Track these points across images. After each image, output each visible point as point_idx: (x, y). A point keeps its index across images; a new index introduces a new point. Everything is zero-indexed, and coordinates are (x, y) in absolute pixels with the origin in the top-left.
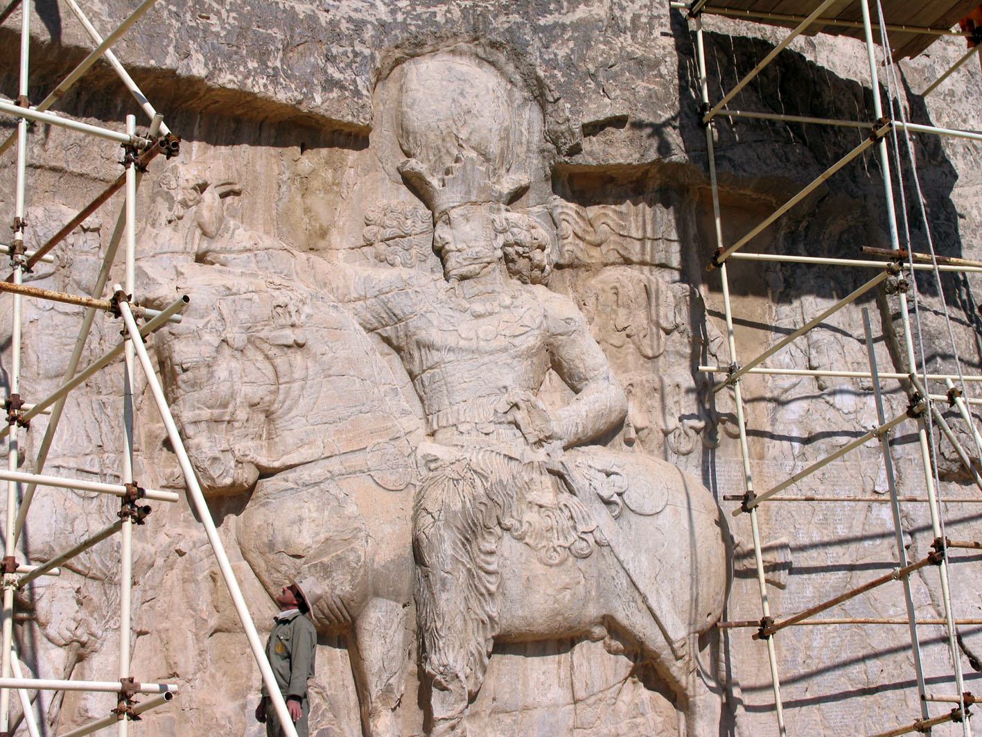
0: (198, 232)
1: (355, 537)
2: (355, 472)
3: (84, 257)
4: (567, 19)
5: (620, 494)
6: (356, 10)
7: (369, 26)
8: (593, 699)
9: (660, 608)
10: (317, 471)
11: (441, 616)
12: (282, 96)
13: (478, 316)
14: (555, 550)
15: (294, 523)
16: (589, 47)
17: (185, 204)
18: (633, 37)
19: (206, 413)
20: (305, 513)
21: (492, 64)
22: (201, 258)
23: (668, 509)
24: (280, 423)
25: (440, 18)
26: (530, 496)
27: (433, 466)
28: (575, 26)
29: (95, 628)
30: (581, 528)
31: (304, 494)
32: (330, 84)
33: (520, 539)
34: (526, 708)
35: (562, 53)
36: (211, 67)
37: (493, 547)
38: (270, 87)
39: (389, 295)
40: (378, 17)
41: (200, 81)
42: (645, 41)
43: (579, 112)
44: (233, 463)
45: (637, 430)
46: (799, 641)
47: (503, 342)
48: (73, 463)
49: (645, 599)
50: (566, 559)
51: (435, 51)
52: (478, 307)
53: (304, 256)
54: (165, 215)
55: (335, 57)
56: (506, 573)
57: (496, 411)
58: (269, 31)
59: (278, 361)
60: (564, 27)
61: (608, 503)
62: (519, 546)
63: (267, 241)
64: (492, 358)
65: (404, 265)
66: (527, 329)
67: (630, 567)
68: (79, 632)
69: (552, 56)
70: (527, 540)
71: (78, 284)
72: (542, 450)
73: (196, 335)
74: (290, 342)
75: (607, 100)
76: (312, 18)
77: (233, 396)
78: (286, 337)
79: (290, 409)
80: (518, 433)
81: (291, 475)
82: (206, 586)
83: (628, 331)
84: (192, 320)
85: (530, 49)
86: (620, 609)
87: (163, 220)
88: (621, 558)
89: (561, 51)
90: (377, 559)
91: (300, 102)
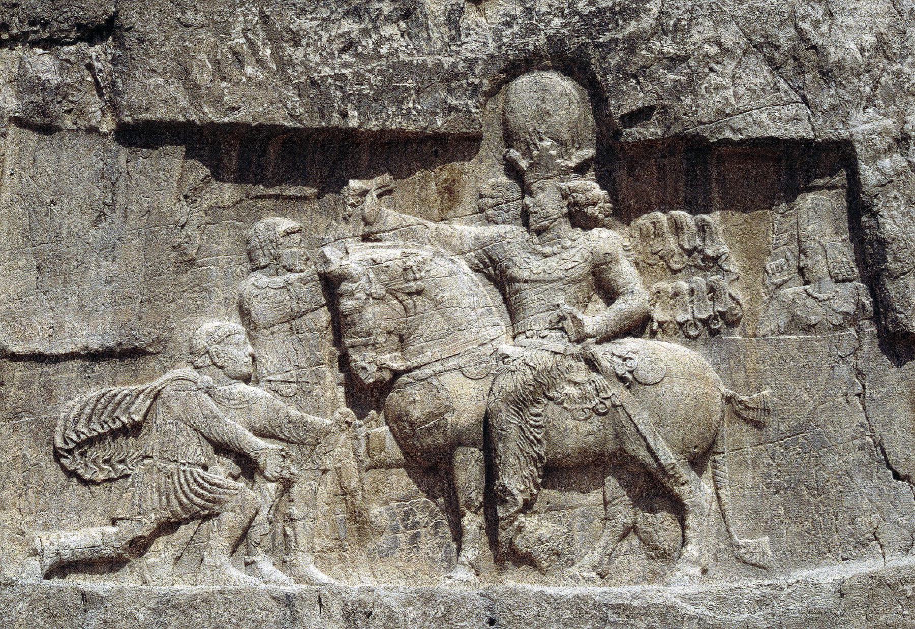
0: (362, 224)
2: (450, 370)
3: (289, 251)
4: (620, 36)
5: (631, 372)
6: (473, 51)
7: (480, 62)
8: (616, 501)
9: (656, 446)
10: (427, 371)
12: (412, 127)
14: (583, 411)
15: (410, 403)
16: (634, 53)
17: (353, 205)
18: (673, 39)
20: (418, 398)
22: (366, 238)
23: (666, 379)
24: (406, 342)
25: (530, 47)
26: (569, 377)
27: (506, 360)
28: (625, 39)
29: (293, 470)
31: (418, 385)
32: (450, 109)
33: (560, 404)
35: (613, 62)
36: (362, 118)
37: (539, 411)
39: (489, 247)
40: (488, 52)
41: (353, 129)
42: (682, 40)
43: (619, 106)
44: (375, 369)
46: (773, 460)
47: (560, 274)
48: (279, 377)
50: (590, 416)
51: (527, 71)
52: (547, 250)
53: (432, 225)
54: (342, 214)
55: (454, 90)
59: (405, 303)
60: (616, 41)
61: (622, 379)
62: (558, 409)
63: (411, 219)
64: (551, 285)
65: (504, 222)
66: (576, 263)
68: (284, 472)
69: (607, 65)
70: (565, 405)
71: (284, 267)
72: (580, 346)
73: (352, 294)
74: (413, 290)
75: (642, 94)
77: (375, 328)
78: (411, 287)
79: (413, 332)
80: (565, 335)
81: (413, 374)
82: (363, 441)
83: (660, 254)
84: (350, 284)
85: (592, 61)
87: (340, 218)
89: (613, 60)
90: (460, 423)
91: (425, 129)
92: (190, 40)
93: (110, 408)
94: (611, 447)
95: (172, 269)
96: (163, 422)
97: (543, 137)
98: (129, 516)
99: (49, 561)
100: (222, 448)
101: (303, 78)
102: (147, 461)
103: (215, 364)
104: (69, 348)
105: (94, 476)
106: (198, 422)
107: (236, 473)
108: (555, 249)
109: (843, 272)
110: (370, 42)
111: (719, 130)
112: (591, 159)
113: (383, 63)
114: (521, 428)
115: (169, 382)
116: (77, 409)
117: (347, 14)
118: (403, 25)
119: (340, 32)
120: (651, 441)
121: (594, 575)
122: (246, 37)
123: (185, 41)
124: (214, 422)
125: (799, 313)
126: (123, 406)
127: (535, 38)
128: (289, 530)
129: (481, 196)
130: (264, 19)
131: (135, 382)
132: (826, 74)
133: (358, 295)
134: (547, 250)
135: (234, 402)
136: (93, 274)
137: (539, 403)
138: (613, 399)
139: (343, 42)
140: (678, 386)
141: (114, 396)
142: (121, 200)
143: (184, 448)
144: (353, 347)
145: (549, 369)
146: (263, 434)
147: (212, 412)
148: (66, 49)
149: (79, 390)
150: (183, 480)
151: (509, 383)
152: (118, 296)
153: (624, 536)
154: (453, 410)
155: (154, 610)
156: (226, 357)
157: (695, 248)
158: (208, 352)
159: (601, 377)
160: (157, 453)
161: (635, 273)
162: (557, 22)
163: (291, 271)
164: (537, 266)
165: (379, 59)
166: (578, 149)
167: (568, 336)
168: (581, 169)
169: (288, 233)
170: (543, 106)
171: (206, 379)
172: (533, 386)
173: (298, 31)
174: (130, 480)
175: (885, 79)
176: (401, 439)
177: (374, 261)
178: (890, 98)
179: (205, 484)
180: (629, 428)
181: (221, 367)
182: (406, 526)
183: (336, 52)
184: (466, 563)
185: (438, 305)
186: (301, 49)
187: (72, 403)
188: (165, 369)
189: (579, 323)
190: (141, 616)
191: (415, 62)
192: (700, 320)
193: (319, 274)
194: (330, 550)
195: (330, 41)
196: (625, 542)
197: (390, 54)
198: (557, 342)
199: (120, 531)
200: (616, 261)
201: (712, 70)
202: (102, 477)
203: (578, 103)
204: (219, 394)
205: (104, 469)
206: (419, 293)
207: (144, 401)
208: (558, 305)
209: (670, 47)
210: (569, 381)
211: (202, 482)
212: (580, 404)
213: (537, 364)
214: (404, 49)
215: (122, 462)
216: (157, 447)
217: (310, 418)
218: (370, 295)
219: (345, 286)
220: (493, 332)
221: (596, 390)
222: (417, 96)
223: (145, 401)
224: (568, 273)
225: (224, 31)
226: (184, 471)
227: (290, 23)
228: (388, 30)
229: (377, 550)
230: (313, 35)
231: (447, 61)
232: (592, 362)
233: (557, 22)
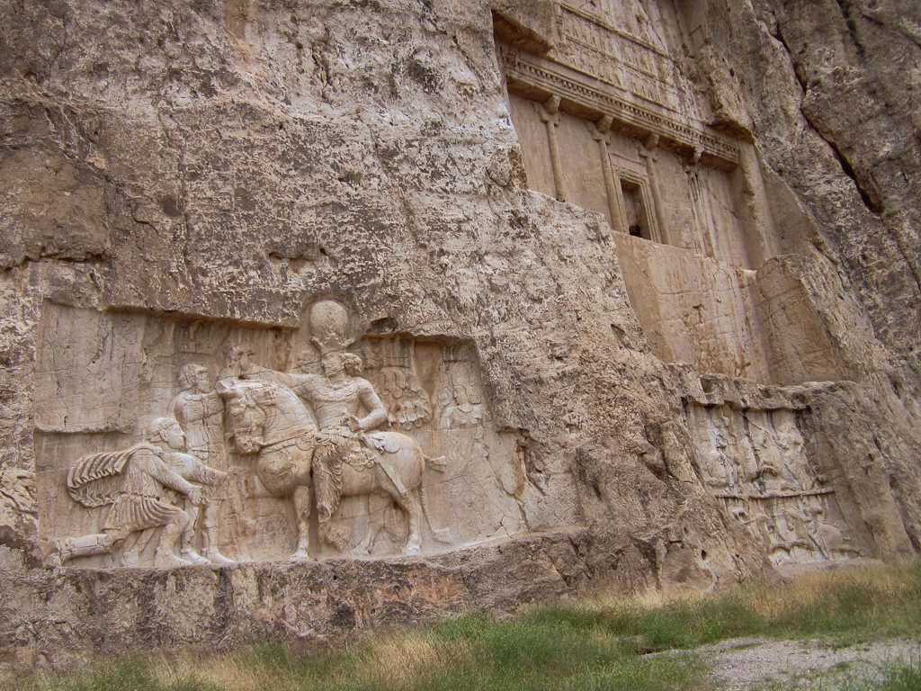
10: (280, 446)
12: (267, 321)
13: (335, 389)
17: (236, 360)
19: (242, 429)
21: (342, 302)
22: (241, 378)
25: (323, 288)
32: (284, 315)
33: (349, 463)
34: (353, 517)
41: (238, 320)
45: (392, 424)
48: (199, 449)
51: (321, 300)
52: (335, 386)
53: (276, 373)
56: (343, 475)
60: (365, 287)
61: (379, 450)
63: (264, 369)
65: (312, 372)
67: (386, 470)
76: (278, 293)
77: (251, 422)
89: (365, 296)
93: (102, 464)
94: (373, 485)
99: (66, 555)
100: (166, 487)
101: (210, 292)
102: (123, 496)
103: (163, 440)
104: (78, 430)
106: (155, 473)
107: (175, 502)
108: (340, 386)
109: (474, 400)
111: (418, 331)
112: (353, 344)
116: (81, 465)
117: (230, 264)
118: (259, 272)
121: (366, 552)
124: (163, 474)
126: (110, 463)
128: (205, 534)
129: (299, 360)
130: (188, 262)
132: (460, 309)
134: (335, 386)
136: (92, 388)
141: (103, 458)
142: (108, 350)
144: (239, 433)
146: (191, 480)
148: (79, 265)
149: (82, 454)
150: (145, 507)
152: (105, 401)
153: (380, 531)
155: (143, 581)
158: (159, 434)
162: (335, 278)
163: (204, 392)
164: (332, 393)
166: (348, 338)
168: (350, 348)
169: (201, 372)
171: (158, 449)
175: (483, 314)
176: (264, 484)
178: (486, 323)
181: (167, 442)
182: (267, 529)
185: (283, 412)
187: (78, 461)
188: (133, 443)
190: (135, 585)
193: (218, 394)
194: (227, 544)
196: (380, 534)
198: (346, 431)
200: (371, 392)
201: (411, 304)
202: (96, 505)
206: (273, 405)
207: (123, 460)
209: (389, 291)
210: (352, 452)
215: (108, 496)
217: (216, 471)
218: (248, 406)
219: (233, 401)
220: (310, 427)
223: (123, 460)
226: (146, 501)
228: (253, 273)
229: (253, 543)
231: (282, 292)
233: (335, 278)
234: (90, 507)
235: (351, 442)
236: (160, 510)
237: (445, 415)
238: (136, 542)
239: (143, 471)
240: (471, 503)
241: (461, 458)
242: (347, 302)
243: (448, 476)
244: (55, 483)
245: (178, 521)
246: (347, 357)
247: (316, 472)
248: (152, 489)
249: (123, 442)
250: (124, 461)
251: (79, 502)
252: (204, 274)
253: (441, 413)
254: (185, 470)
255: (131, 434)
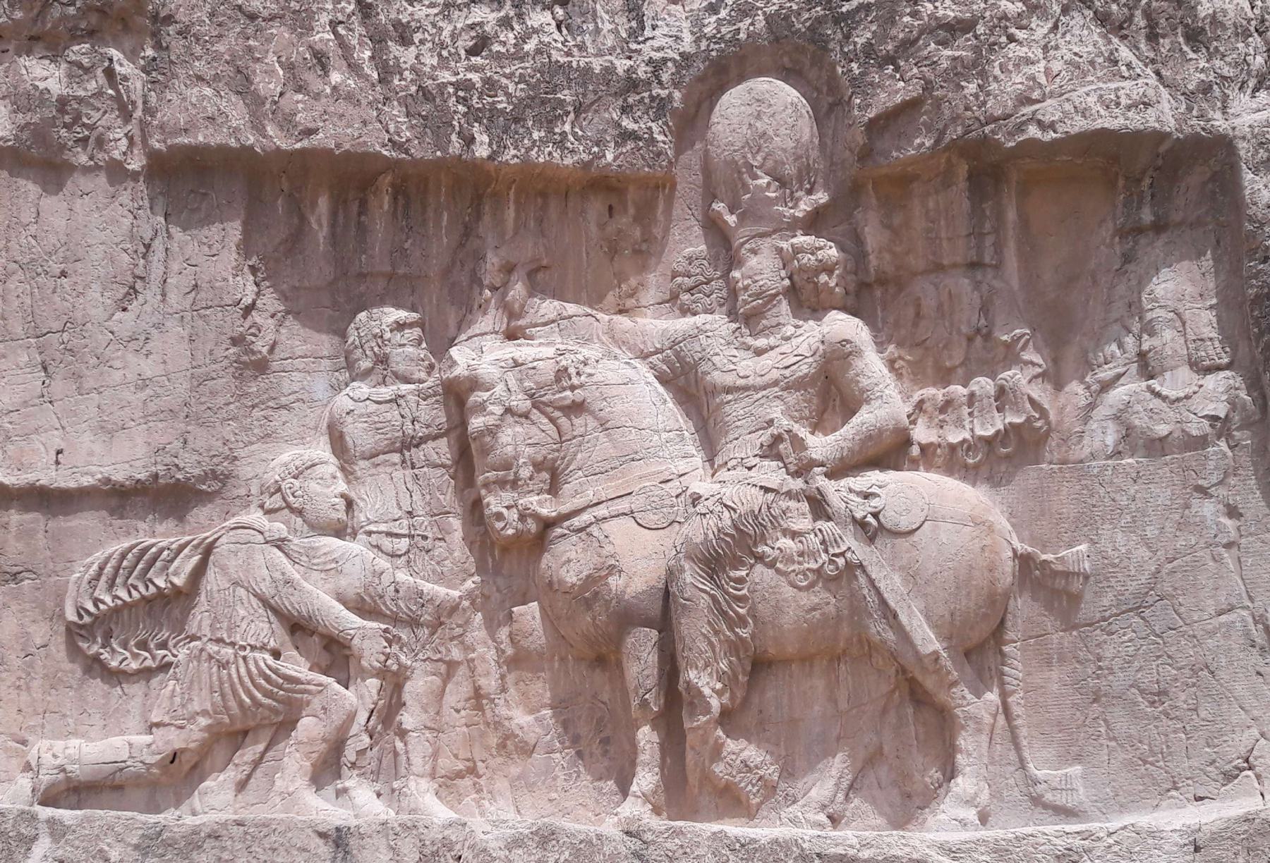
1: (610, 574)
5: (875, 515)
9: (911, 624)
11: (683, 639)
12: (568, 161)
14: (805, 575)
30: (831, 551)
37: (744, 573)
38: (555, 154)
47: (775, 374)
49: (895, 616)
57: (762, 444)
58: (559, 95)
61: (861, 524)
62: (771, 572)
66: (800, 358)
67: (881, 586)
86: (872, 626)
88: (874, 577)
90: (628, 590)
91: (590, 163)
92: (255, 38)
95: (232, 370)
96: (215, 588)
97: (759, 173)
98: (167, 720)
103: (289, 506)
105: (124, 663)
106: (266, 588)
110: (511, 35)
113: (527, 65)
114: (713, 597)
115: (223, 531)
119: (469, 22)
120: (903, 618)
122: (335, 33)
123: (248, 39)
124: (285, 590)
125: (1137, 422)
127: (750, 21)
131: (184, 534)
133: (491, 408)
135: (316, 561)
137: (743, 564)
138: (848, 555)
139: (473, 38)
140: (946, 533)
143: (244, 625)
145: (756, 512)
147: (283, 574)
149: (100, 544)
150: (243, 670)
151: (698, 530)
154: (620, 571)
156: (306, 497)
157: (978, 331)
158: (279, 490)
159: (830, 524)
160: (206, 630)
161: (885, 371)
165: (522, 59)
167: (785, 466)
170: (758, 124)
171: (278, 528)
172: (732, 536)
173: (409, 22)
174: (172, 670)
177: (515, 361)
179: (273, 676)
180: (872, 599)
181: (300, 512)
183: (463, 53)
184: (639, 794)
186: (413, 48)
189: (798, 443)
191: (574, 65)
192: (981, 438)
195: (454, 36)
197: (538, 51)
198: (772, 474)
199: (154, 742)
200: (858, 352)
202: (134, 665)
203: (810, 117)
204: (295, 548)
205: (139, 654)
208: (772, 421)
211: (268, 672)
212: (799, 563)
213: (740, 505)
214: (560, 45)
215: (163, 646)
216: (206, 623)
221: (823, 542)
222: (577, 117)
224: (787, 372)
225: (302, 22)
226: (244, 658)
227: (399, 12)
228: (539, 18)
230: (429, 28)
232: (819, 502)
234: (124, 672)
235: (784, 504)
236: (281, 681)
237: (1101, 412)
238: (230, 760)
239: (236, 583)
240: (1159, 694)
241: (1143, 552)
242: (812, 74)
243: (1088, 610)
244: (43, 612)
245: (324, 708)
246: (797, 250)
247: (673, 589)
248: (263, 629)
249: (200, 514)
250: (196, 559)
251: (96, 659)
252: (404, 35)
253: (1091, 406)
254: (343, 582)
255: (217, 493)
